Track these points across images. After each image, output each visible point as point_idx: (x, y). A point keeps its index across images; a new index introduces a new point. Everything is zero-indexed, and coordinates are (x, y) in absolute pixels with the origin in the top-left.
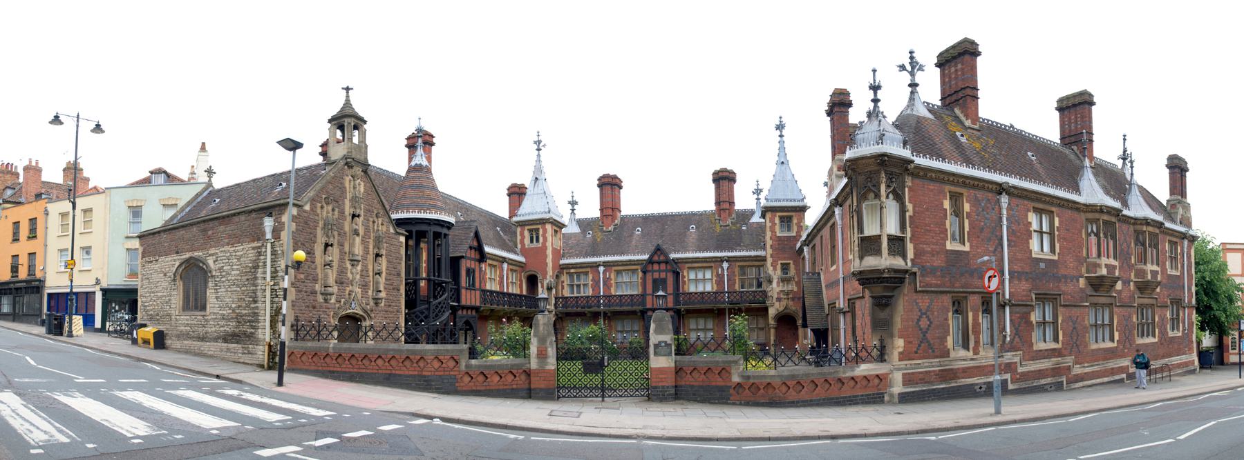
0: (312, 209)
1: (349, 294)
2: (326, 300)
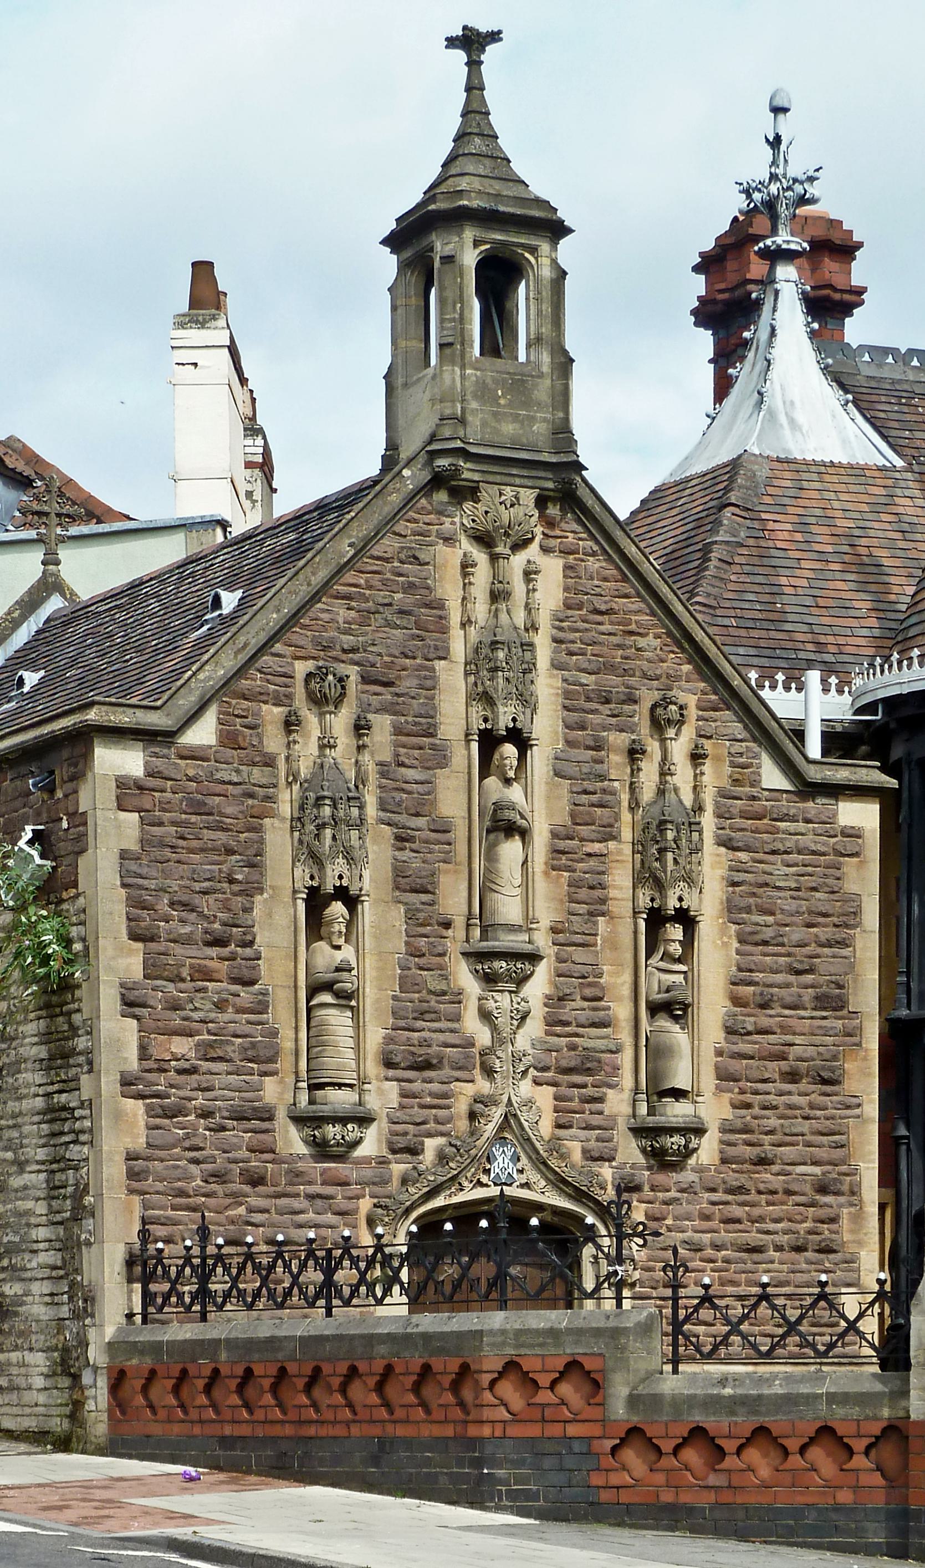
0: (228, 739)
1: (472, 1116)
2: (322, 1150)
